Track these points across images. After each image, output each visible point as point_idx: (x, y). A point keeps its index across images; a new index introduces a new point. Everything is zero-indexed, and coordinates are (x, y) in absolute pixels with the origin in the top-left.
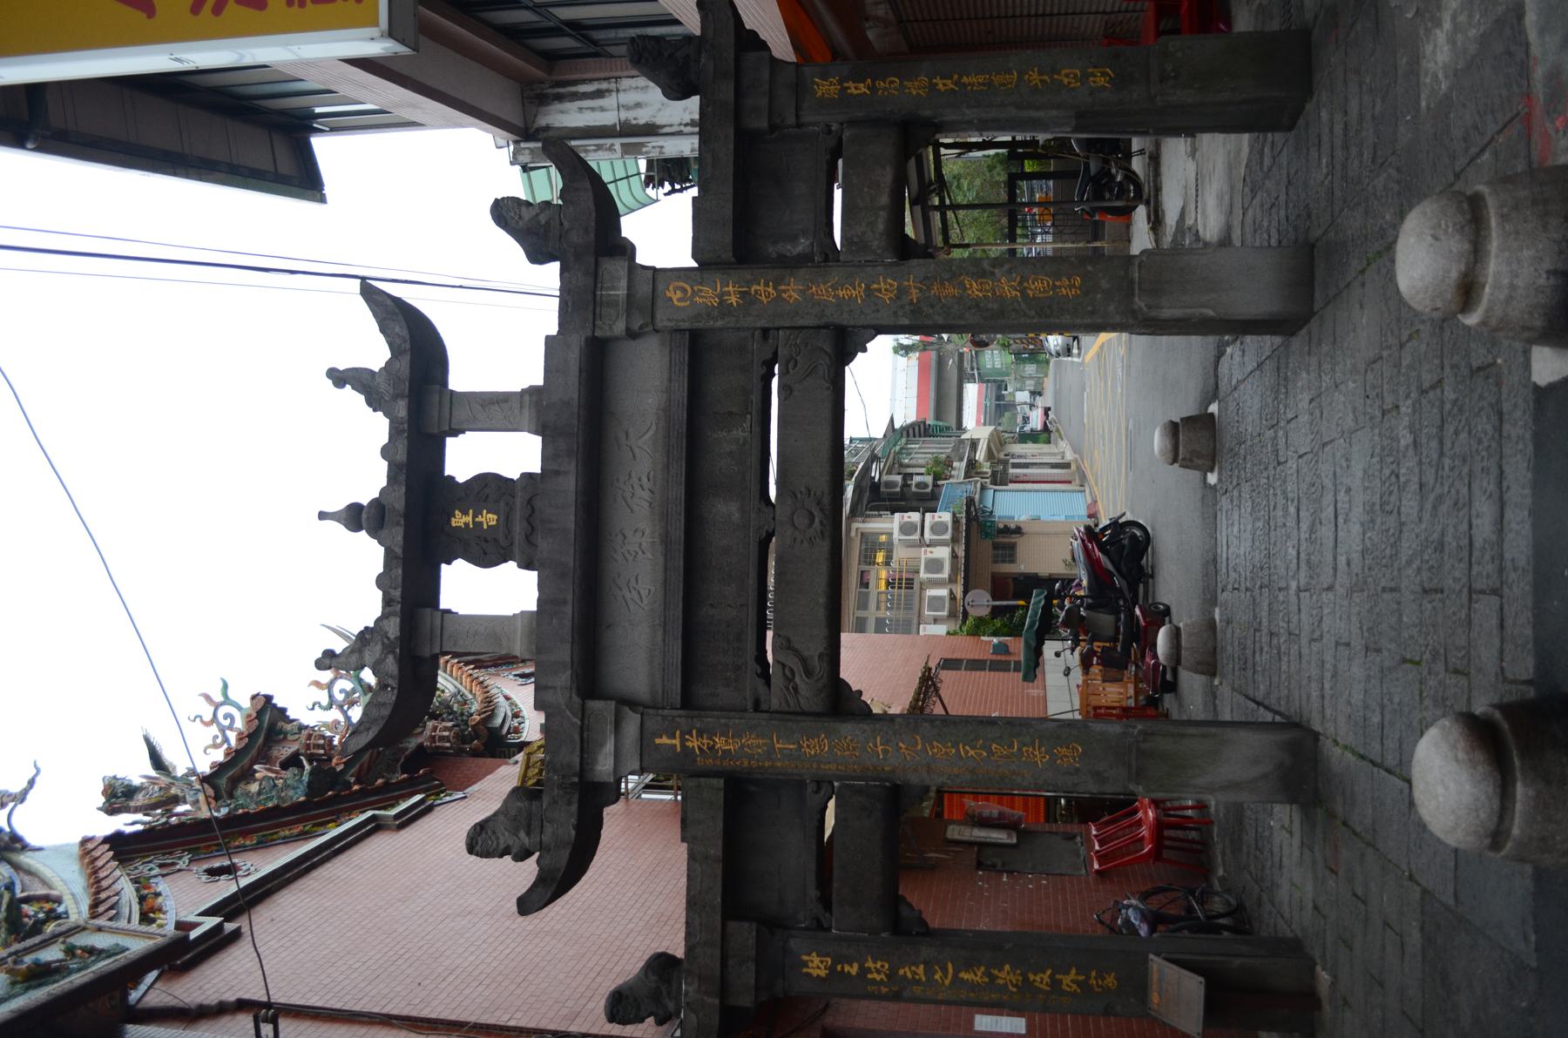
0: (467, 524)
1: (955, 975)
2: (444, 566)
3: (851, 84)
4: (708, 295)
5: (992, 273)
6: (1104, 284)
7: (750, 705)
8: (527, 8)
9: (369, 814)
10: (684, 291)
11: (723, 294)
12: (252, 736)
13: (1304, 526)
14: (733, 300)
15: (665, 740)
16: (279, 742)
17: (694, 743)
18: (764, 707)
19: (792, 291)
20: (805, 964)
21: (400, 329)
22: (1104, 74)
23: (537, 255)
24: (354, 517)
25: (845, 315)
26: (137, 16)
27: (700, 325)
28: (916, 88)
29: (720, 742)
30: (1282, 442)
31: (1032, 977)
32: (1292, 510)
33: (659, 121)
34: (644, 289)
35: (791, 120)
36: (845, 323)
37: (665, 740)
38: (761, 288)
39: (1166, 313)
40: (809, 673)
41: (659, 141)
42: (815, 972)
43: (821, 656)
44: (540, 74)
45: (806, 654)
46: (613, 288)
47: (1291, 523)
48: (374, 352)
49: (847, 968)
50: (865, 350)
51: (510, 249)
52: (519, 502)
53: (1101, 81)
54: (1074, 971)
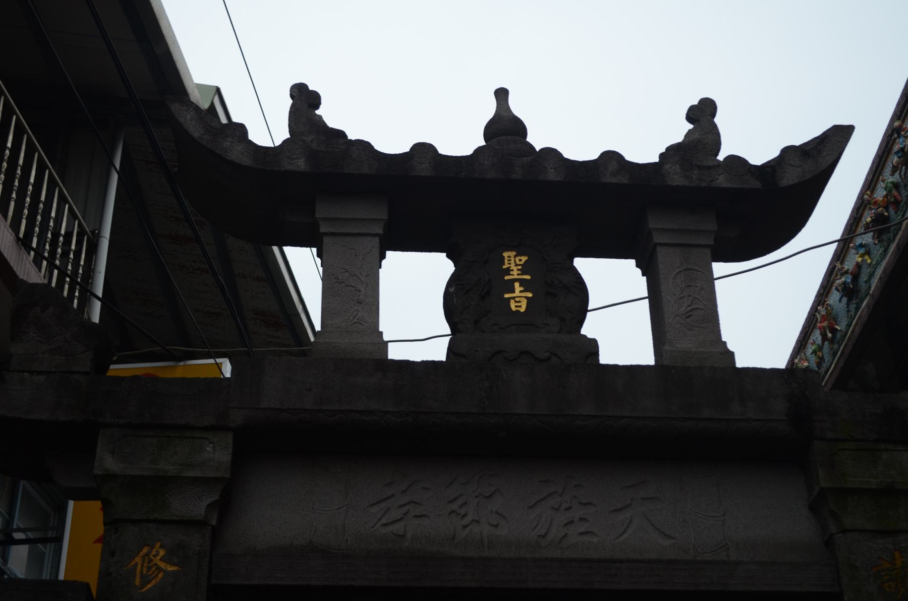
21: (789, 178)
48: (752, 138)
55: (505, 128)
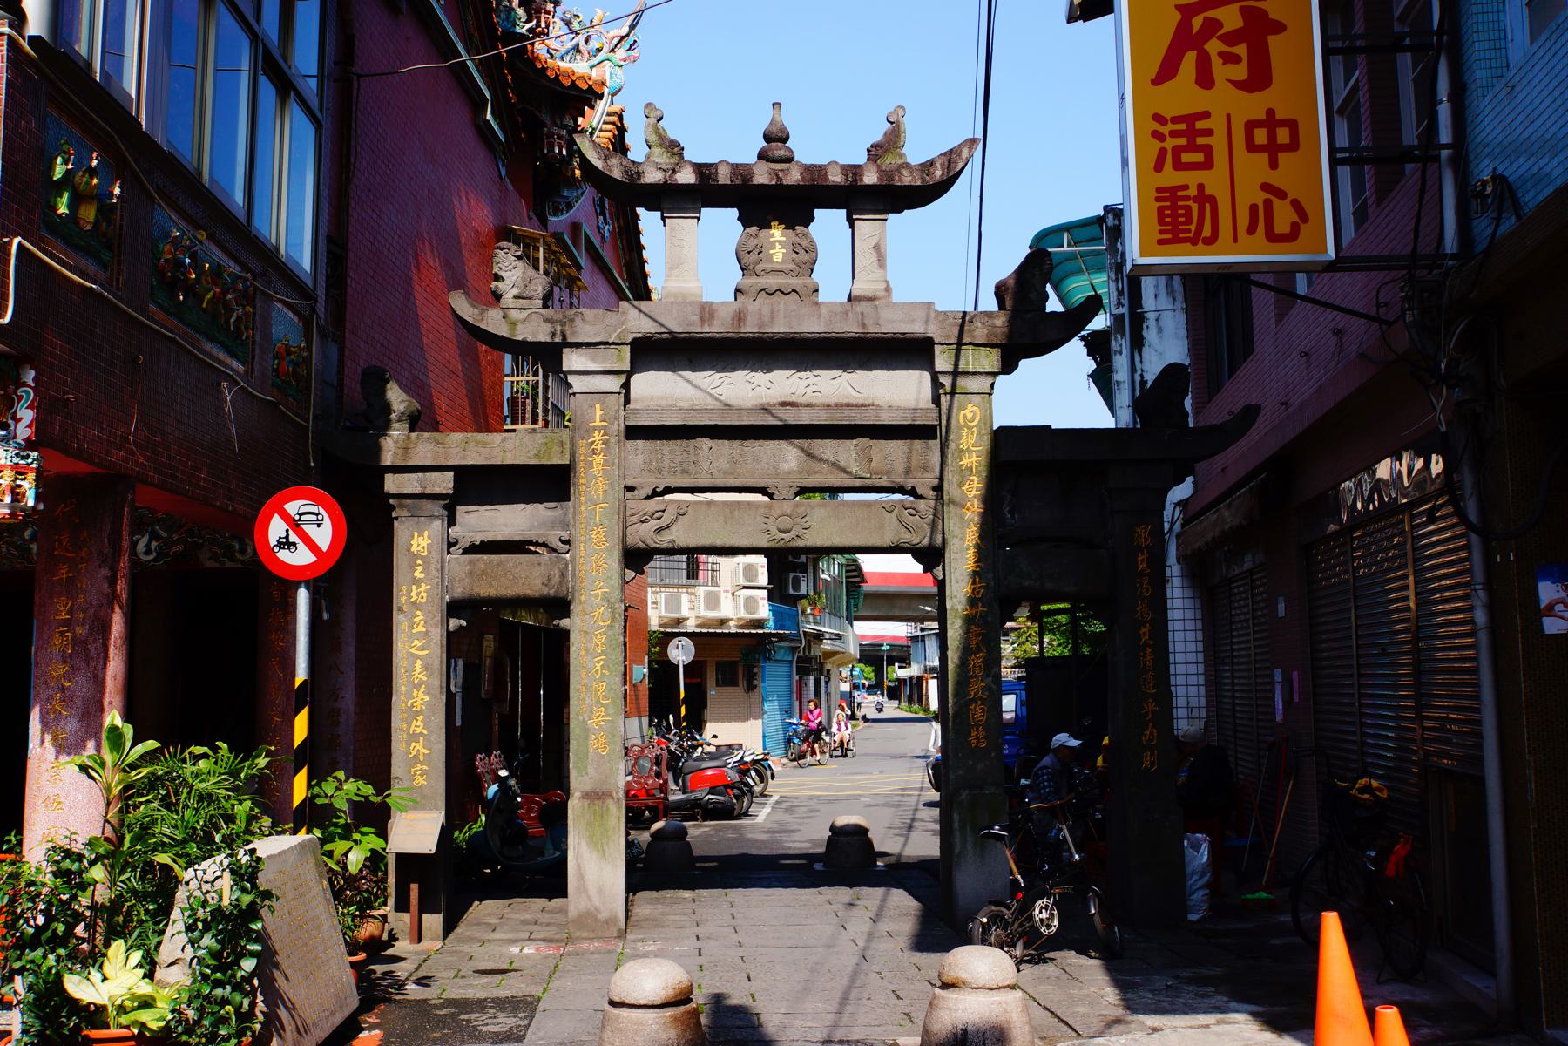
1: (418, 657)
2: (734, 212)
6: (980, 766)
7: (629, 483)
10: (973, 419)
11: (968, 451)
14: (965, 461)
15: (599, 413)
17: (597, 437)
18: (629, 495)
22: (1152, 764)
26: (1153, 74)
29: (599, 459)
31: (420, 718)
33: (1145, 350)
37: (599, 413)
40: (659, 531)
41: (1126, 351)
42: (414, 542)
43: (672, 541)
45: (674, 528)
48: (918, 149)
49: (420, 568)
52: (794, 282)
55: (776, 137)
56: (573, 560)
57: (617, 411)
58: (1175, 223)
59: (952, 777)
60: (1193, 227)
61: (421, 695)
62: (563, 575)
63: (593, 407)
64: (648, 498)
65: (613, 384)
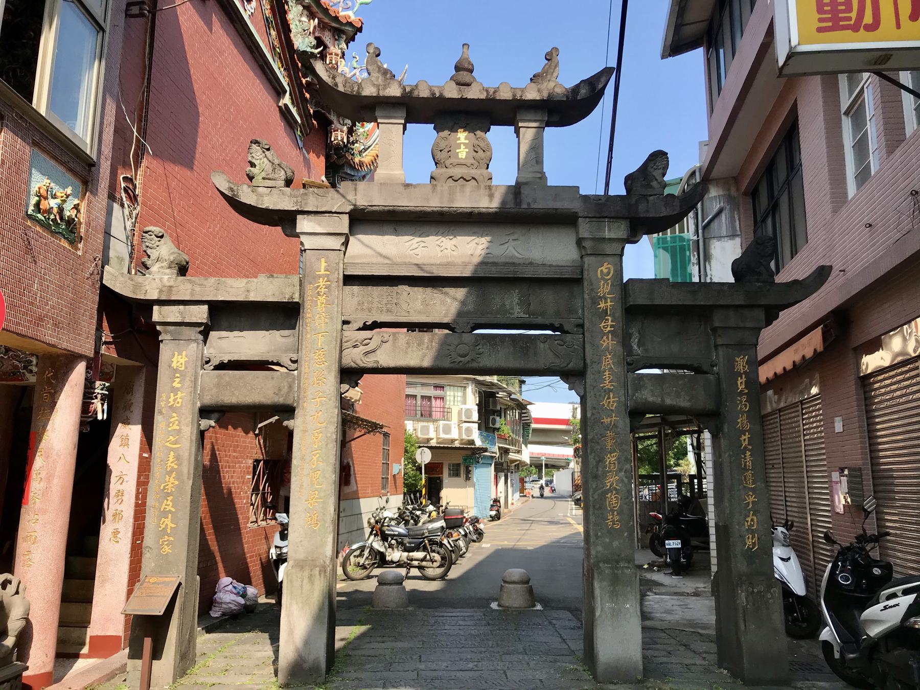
0: (459, 139)
3: (744, 379)
4: (605, 288)
5: (621, 470)
6: (616, 544)
8: (788, 176)
9: (287, 88)
10: (608, 273)
12: (336, 19)
13: (459, 674)
14: (602, 305)
15: (323, 265)
16: (334, 36)
17: (321, 282)
18: (345, 327)
19: (608, 342)
20: (180, 354)
22: (754, 544)
23: (630, 180)
24: (463, 68)
25: (593, 377)
27: (586, 284)
28: (742, 421)
30: (514, 658)
31: (170, 498)
32: (471, 665)
34: (610, 249)
35: (720, 341)
36: (588, 376)
38: (610, 323)
39: (596, 585)
40: (367, 353)
42: (175, 360)
43: (377, 362)
44: (743, 188)
45: (378, 352)
46: (609, 230)
47: (462, 665)
49: (177, 380)
50: (570, 389)
51: (634, 165)
53: (749, 542)
54: (173, 526)
56: (299, 374)
57: (338, 264)
58: (835, 12)
59: (593, 552)
60: (853, 15)
61: (172, 480)
62: (290, 387)
63: (319, 260)
64: (359, 329)
65: (336, 243)
